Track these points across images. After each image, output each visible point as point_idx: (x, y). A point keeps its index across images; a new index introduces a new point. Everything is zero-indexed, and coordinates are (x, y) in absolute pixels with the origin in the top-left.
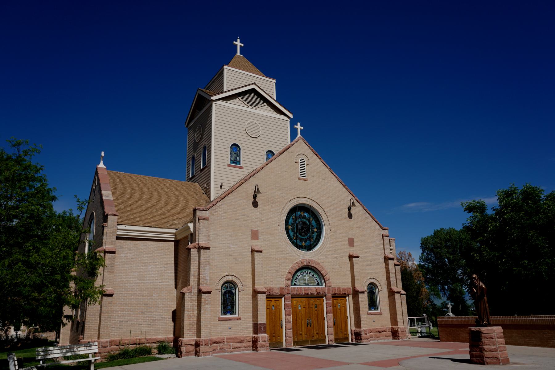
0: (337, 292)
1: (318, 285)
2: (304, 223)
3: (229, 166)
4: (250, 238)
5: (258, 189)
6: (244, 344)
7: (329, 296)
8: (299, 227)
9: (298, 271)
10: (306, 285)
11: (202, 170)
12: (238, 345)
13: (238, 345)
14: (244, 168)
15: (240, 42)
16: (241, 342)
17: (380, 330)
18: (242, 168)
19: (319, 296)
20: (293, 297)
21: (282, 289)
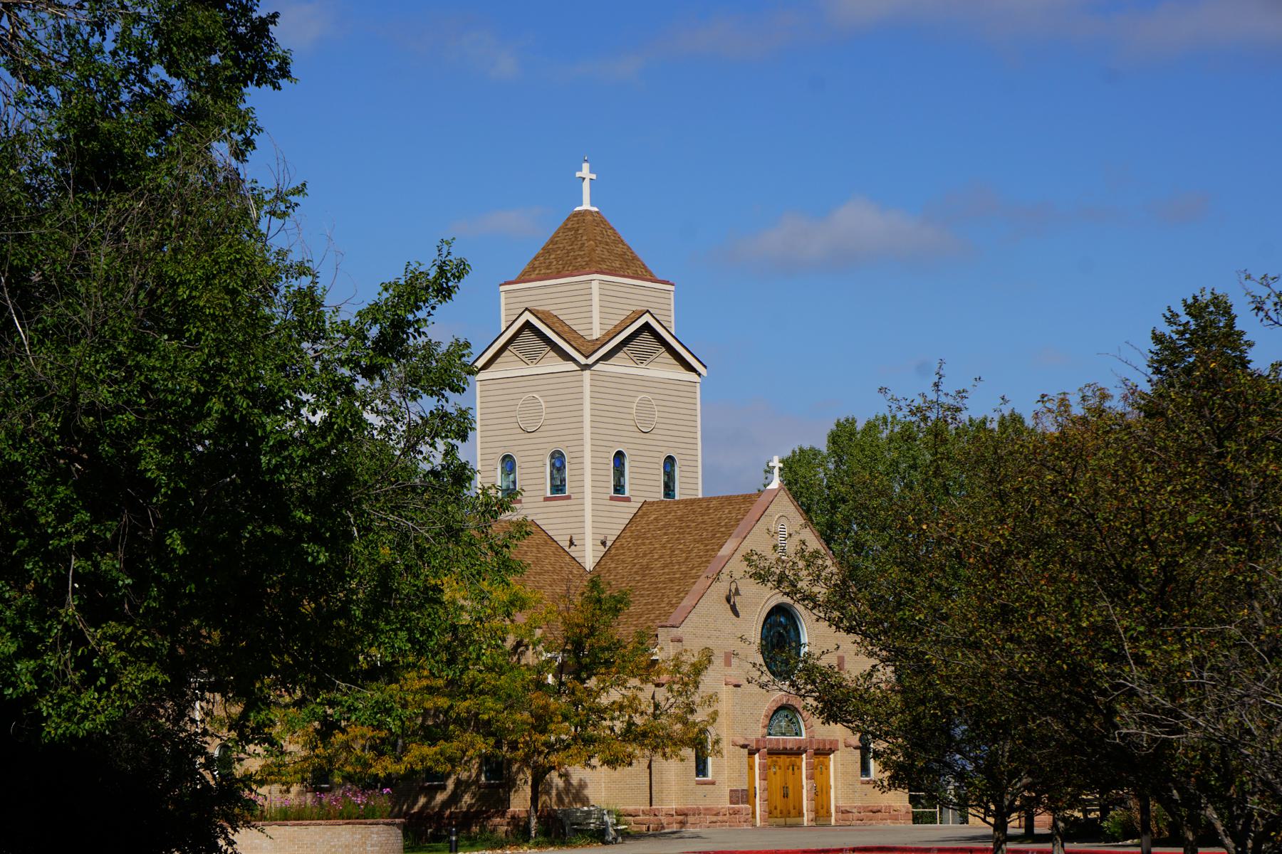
0: (821, 747)
1: (797, 734)
2: (780, 635)
3: (612, 499)
4: (723, 664)
5: (737, 590)
6: (720, 818)
7: (811, 751)
8: (775, 641)
9: (776, 712)
10: (784, 734)
11: (547, 499)
12: (714, 819)
13: (714, 819)
14: (633, 499)
15: (591, 172)
16: (717, 814)
17: (875, 809)
18: (628, 500)
19: (798, 752)
20: (772, 753)
21: (758, 741)
